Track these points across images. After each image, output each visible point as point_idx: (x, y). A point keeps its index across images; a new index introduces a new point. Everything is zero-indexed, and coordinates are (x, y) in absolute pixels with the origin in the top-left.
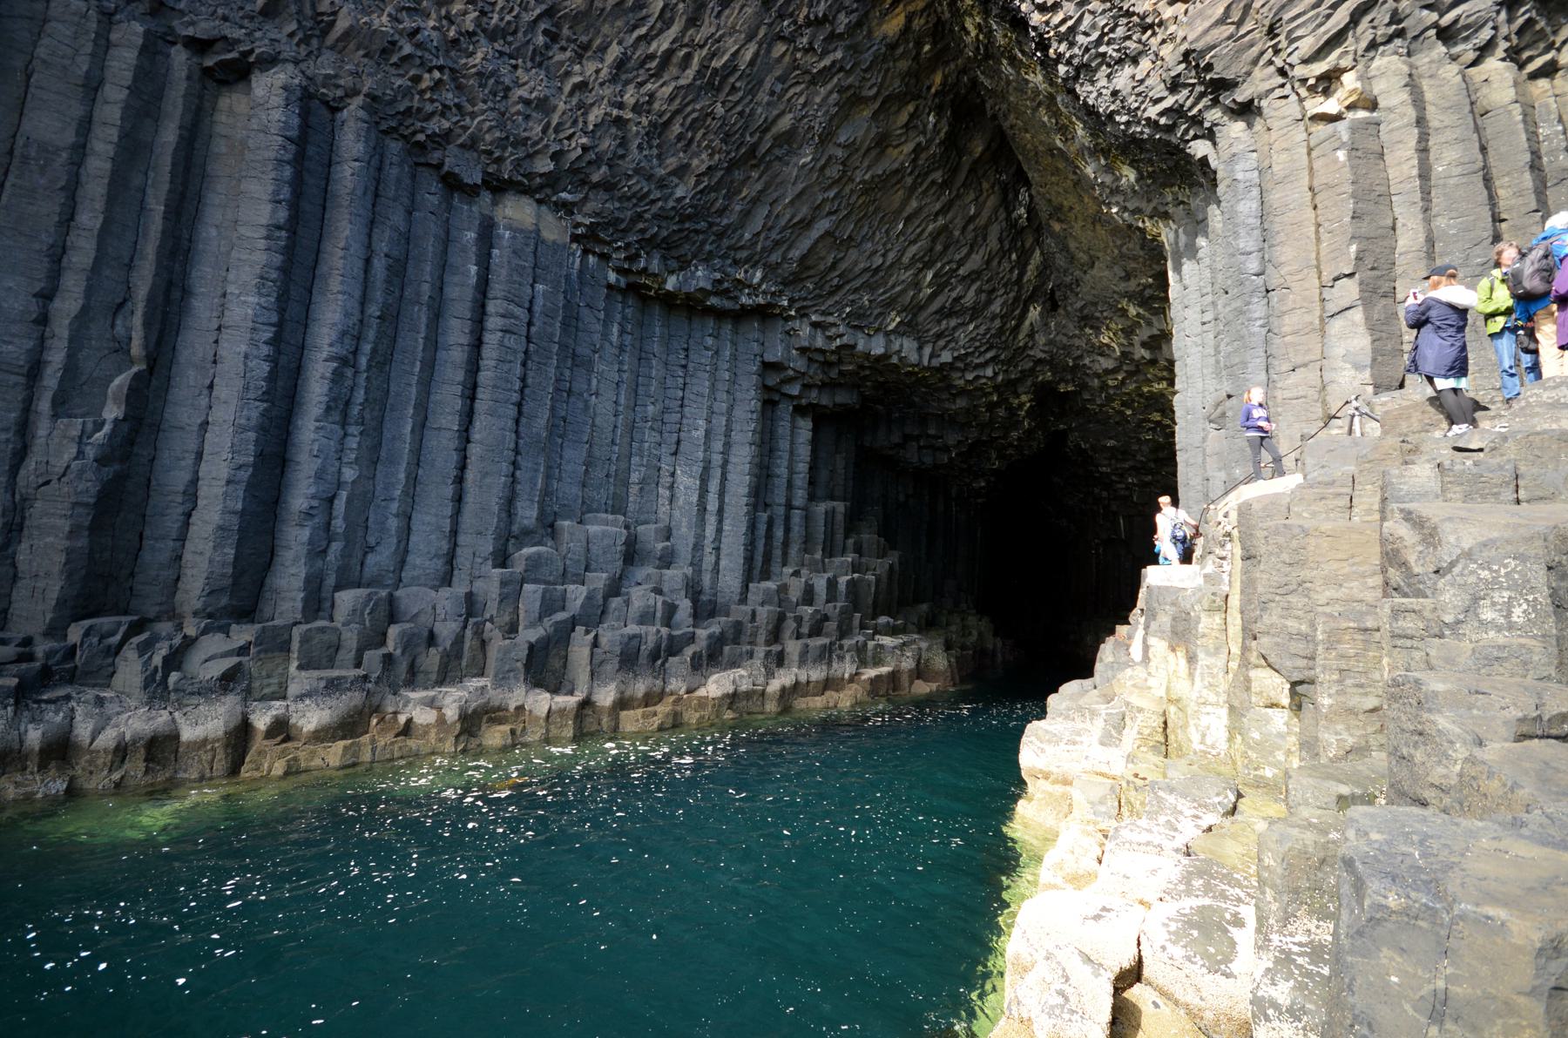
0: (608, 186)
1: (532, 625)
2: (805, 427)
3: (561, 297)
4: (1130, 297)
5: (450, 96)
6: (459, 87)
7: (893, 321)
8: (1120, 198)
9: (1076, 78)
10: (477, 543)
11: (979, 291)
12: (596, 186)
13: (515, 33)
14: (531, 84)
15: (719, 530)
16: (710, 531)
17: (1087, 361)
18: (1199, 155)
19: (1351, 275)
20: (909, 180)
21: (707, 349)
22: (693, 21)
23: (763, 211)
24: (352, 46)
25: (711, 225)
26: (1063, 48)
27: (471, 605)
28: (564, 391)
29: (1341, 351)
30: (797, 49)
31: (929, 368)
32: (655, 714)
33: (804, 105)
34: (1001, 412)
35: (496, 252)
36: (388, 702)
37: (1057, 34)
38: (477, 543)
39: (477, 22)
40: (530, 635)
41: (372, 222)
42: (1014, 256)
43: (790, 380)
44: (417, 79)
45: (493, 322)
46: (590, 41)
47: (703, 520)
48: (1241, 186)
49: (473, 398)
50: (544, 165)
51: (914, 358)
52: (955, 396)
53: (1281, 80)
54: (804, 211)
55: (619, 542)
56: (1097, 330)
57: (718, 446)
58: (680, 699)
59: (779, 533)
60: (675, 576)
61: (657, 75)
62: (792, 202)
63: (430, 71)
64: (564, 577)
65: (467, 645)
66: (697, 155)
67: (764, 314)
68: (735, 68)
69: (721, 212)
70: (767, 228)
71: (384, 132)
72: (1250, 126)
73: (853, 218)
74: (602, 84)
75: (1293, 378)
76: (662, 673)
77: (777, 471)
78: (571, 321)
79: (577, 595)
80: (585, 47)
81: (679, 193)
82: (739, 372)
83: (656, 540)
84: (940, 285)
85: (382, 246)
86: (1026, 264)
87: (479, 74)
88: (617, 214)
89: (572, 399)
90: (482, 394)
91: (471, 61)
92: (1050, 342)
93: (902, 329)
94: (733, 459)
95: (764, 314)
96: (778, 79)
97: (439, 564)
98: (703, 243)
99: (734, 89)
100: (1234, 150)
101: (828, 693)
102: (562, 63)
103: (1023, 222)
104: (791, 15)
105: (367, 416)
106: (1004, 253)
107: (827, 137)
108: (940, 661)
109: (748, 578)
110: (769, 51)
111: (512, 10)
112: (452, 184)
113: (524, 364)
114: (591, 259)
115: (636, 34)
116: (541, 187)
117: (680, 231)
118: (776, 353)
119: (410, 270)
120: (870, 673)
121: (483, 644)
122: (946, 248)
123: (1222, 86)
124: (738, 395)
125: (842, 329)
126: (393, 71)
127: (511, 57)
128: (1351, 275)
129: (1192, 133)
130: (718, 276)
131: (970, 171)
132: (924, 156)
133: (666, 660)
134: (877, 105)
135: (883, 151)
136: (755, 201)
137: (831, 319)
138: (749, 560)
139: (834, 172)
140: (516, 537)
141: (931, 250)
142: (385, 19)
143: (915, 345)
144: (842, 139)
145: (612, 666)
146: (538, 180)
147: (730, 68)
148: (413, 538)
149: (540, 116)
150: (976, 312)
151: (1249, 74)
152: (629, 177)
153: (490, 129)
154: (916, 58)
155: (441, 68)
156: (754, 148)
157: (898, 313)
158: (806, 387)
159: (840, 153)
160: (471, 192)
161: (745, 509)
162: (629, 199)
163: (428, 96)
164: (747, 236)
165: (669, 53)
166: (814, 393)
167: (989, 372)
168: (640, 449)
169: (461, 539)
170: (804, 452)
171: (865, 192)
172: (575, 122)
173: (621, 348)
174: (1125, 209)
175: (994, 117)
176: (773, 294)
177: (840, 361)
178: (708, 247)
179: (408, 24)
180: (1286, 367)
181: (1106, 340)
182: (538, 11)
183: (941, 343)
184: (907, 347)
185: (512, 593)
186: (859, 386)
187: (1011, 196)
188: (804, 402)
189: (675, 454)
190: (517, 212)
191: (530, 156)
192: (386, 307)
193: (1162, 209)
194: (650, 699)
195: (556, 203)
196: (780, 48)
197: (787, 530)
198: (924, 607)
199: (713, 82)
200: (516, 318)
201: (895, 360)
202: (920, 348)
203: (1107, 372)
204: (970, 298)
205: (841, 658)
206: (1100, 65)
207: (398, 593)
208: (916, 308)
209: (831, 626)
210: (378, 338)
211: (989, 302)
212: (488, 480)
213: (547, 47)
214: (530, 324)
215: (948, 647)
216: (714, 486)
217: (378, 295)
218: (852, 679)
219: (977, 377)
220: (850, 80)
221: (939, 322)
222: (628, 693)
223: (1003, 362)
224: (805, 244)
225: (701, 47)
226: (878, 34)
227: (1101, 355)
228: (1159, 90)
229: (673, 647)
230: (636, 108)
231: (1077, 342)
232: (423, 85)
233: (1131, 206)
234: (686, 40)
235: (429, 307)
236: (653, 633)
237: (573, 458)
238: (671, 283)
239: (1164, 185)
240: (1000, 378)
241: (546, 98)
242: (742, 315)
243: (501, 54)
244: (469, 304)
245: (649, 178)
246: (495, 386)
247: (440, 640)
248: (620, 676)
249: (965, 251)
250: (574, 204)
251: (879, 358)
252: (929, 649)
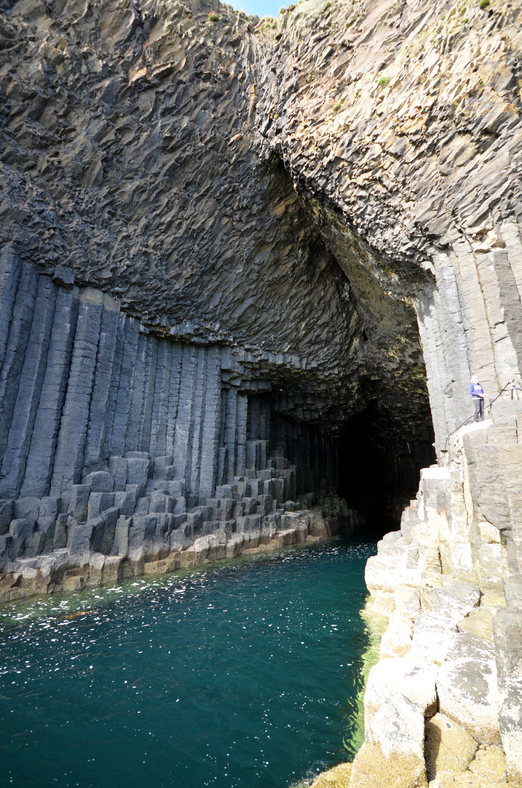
0: (139, 284)
1: (95, 516)
2: (244, 401)
3: (115, 338)
4: (402, 334)
5: (59, 241)
6: (63, 237)
7: (287, 347)
8: (392, 288)
9: (366, 234)
10: (65, 471)
11: (329, 332)
12: (134, 284)
13: (93, 212)
14: (101, 236)
15: (200, 458)
16: (195, 459)
17: (383, 365)
18: (426, 269)
19: (503, 322)
20: (291, 280)
21: (191, 363)
22: (183, 208)
23: (218, 296)
24: (8, 218)
25: (193, 302)
26: (359, 221)
27: (60, 506)
28: (115, 387)
29: (503, 358)
30: (233, 221)
31: (306, 370)
32: (165, 564)
33: (238, 246)
34: (344, 391)
35: (80, 317)
36: (8, 566)
37: (356, 215)
38: (65, 471)
39: (74, 208)
40: (93, 521)
41: (14, 303)
42: (344, 315)
43: (235, 378)
44: (41, 234)
45: (78, 352)
46: (132, 217)
47: (191, 453)
48: (447, 282)
49: (65, 392)
50: (107, 274)
51: (298, 365)
53: (460, 235)
54: (239, 295)
55: (145, 467)
56: (387, 349)
57: (198, 413)
58: (179, 554)
59: (232, 458)
60: (176, 484)
61: (165, 232)
62: (233, 291)
63: (49, 230)
64: (114, 487)
65: (57, 529)
66: (185, 269)
67: (221, 345)
68: (204, 229)
69: (198, 296)
70: (221, 303)
71: (24, 259)
72: (448, 255)
73: (264, 298)
74: (137, 236)
75: (482, 372)
76: (169, 540)
77: (230, 425)
78: (120, 351)
79: (121, 497)
80: (129, 219)
81: (176, 287)
82: (208, 374)
83: (165, 465)
84: (309, 329)
85: (19, 314)
86: (350, 319)
87: (74, 231)
88: (144, 298)
89: (120, 391)
90: (71, 390)
91: (70, 225)
92: (365, 356)
93: (291, 351)
94: (206, 420)
95: (221, 345)
96: (225, 234)
97: (43, 484)
98: (189, 311)
99: (203, 238)
100: (442, 266)
101: (261, 546)
102: (117, 227)
103: (347, 299)
104: (230, 205)
105: (6, 403)
106: (339, 314)
107: (249, 261)
108: (320, 524)
109: (216, 484)
110: (220, 221)
111: (92, 202)
112: (58, 283)
113: (94, 374)
114: (131, 320)
115: (154, 213)
116: (105, 285)
117: (177, 305)
118: (227, 365)
119: (34, 326)
120: (283, 533)
121: (67, 528)
122: (311, 311)
123: (433, 238)
124: (209, 386)
125: (261, 352)
126: (29, 230)
127: (91, 223)
128: (503, 322)
129: (422, 258)
130: (197, 327)
131: (321, 275)
132: (297, 269)
133: (171, 532)
134: (273, 246)
135: (277, 267)
136: (215, 290)
137: (255, 347)
138: (216, 473)
139: (254, 276)
140: (87, 466)
141: (304, 312)
142: (26, 205)
143: (298, 359)
144: (257, 261)
145: (140, 537)
146: (104, 281)
147: (201, 229)
148: (28, 470)
149: (105, 251)
150: (327, 342)
151: (445, 232)
152: (151, 280)
153: (79, 257)
154: (291, 224)
155: (54, 229)
156: (214, 266)
157: (289, 344)
158: (244, 381)
159: (256, 268)
160: (69, 287)
161: (213, 446)
162: (151, 290)
163: (47, 241)
164: (211, 307)
165: (170, 223)
166: (248, 385)
167: (336, 371)
168: (157, 416)
169: (56, 469)
170: (244, 415)
171: (270, 286)
172: (123, 254)
173: (147, 364)
174: (395, 293)
175: (330, 251)
176: (225, 335)
177: (261, 368)
178: (191, 313)
179: (38, 208)
180: (478, 366)
181: (392, 355)
182: (105, 203)
183: (311, 357)
184: (294, 360)
185: (83, 498)
186: (270, 380)
187: (340, 287)
188: (243, 389)
189: (175, 418)
190: (92, 297)
191: (100, 270)
192: (19, 345)
193: (412, 293)
194: (162, 555)
195: (113, 293)
196: (225, 220)
197: (236, 456)
198: (310, 495)
199: (193, 235)
200: (90, 350)
201: (288, 366)
202: (301, 360)
203: (394, 370)
204: (324, 336)
205: (267, 525)
206: (377, 228)
207: (17, 502)
208: (297, 341)
209: (261, 508)
210: (14, 362)
211: (334, 337)
212: (73, 436)
213: (110, 219)
214: (98, 353)
215: (324, 516)
216: (196, 434)
217: (15, 340)
218: (273, 537)
219: (330, 374)
220: (260, 235)
221: (309, 347)
222: (149, 552)
223: (342, 366)
225: (187, 219)
226: (272, 214)
227: (390, 361)
228: (405, 240)
229: (175, 524)
230: (155, 247)
231: (378, 356)
232: (45, 236)
233: (397, 291)
234: (179, 216)
235: (43, 345)
236: (163, 517)
237: (120, 422)
238: (173, 331)
239: (412, 282)
240: (342, 374)
241: (109, 243)
242: (209, 346)
243: (86, 222)
244: (65, 344)
245: (161, 280)
246: (78, 385)
247: (41, 527)
248: (145, 543)
249: (320, 313)
250: (122, 293)
251: (280, 366)
252: (314, 517)
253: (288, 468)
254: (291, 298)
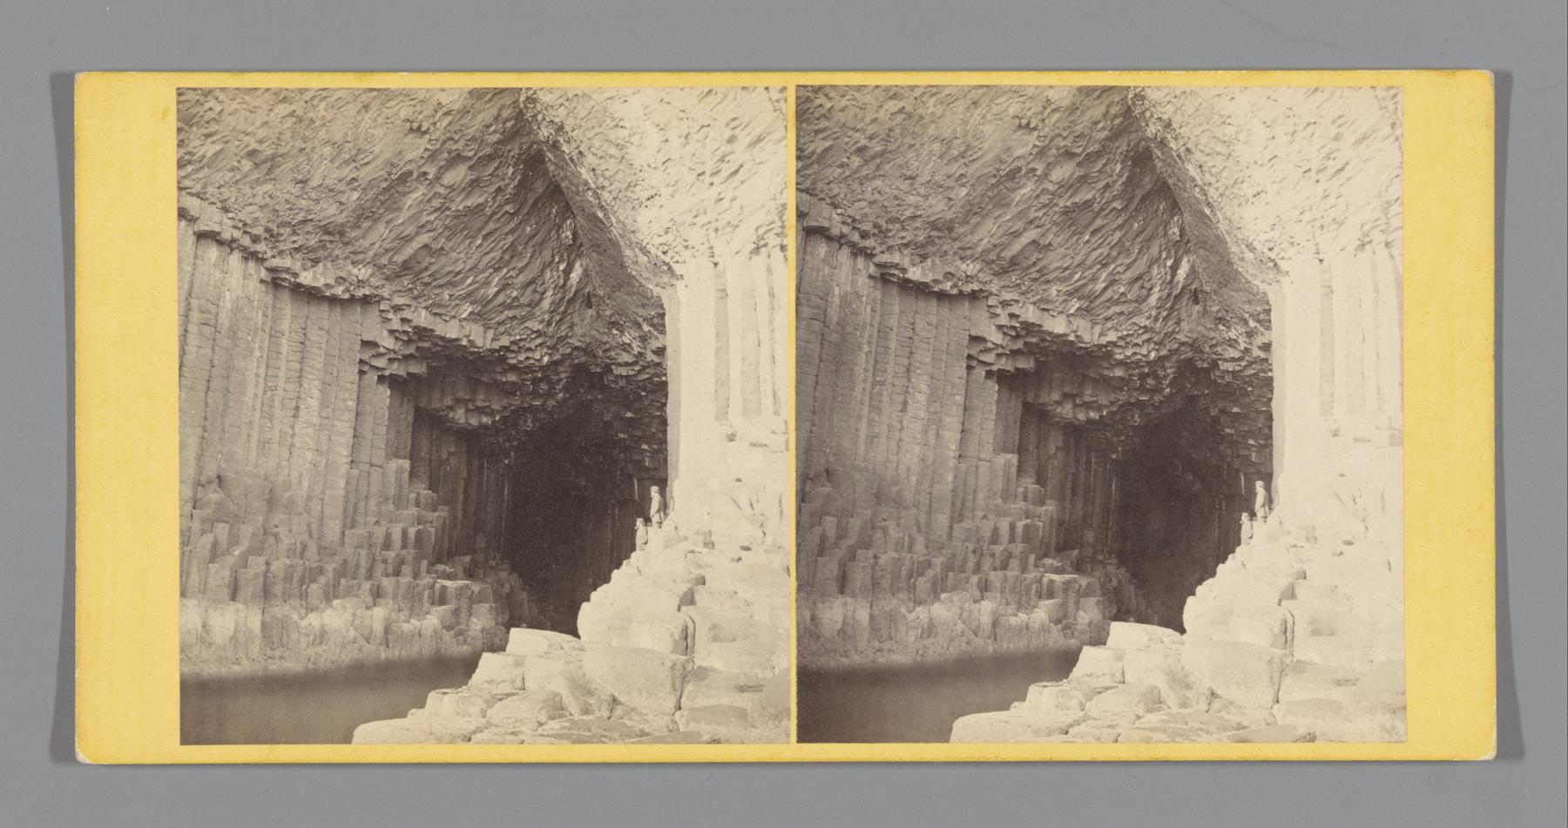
2: (385, 392)
166: (395, 365)
171: (455, 218)
198: (467, 559)
224: (408, 251)
253: (435, 510)
254: (485, 238)
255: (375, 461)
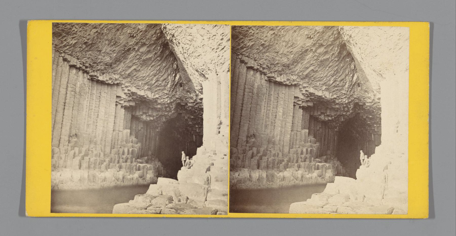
43: (300, 100)
52: (335, 105)
131: (343, 58)
166: (304, 103)
167: (344, 100)
224: (307, 72)
253: (316, 143)
254: (329, 67)
255: (298, 130)
